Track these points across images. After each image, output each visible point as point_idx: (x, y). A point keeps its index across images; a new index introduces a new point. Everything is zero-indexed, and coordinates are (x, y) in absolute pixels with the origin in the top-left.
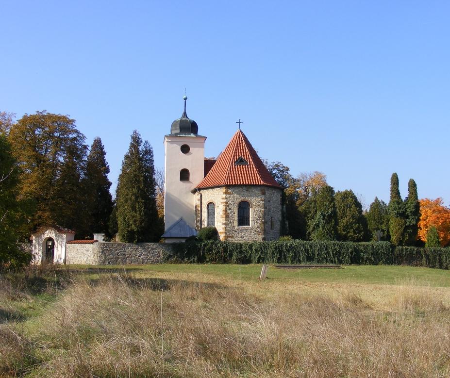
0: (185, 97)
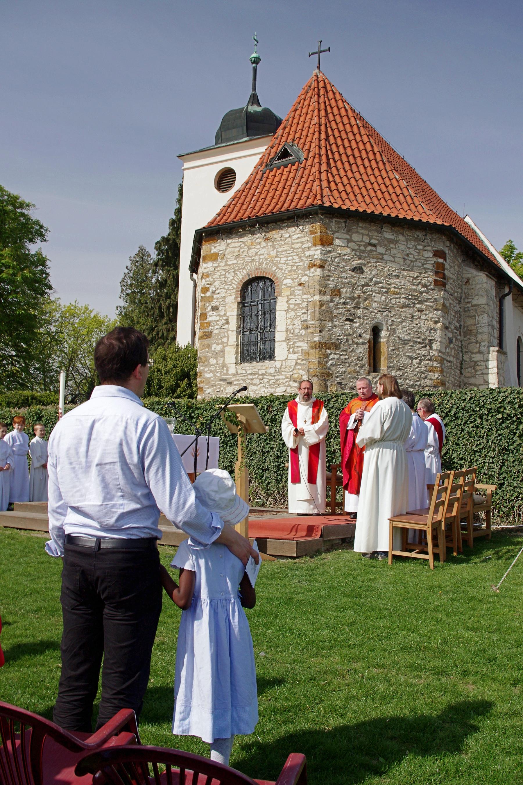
0: (254, 55)
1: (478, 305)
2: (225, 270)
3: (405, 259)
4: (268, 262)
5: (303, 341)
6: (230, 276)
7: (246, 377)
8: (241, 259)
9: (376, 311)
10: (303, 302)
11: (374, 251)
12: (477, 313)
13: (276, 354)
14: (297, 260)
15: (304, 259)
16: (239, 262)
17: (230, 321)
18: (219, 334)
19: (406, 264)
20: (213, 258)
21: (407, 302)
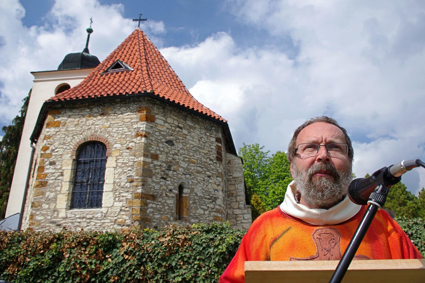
1: (237, 177)
2: (65, 134)
3: (199, 140)
4: (102, 130)
5: (128, 191)
6: (69, 139)
7: (74, 220)
8: (80, 127)
9: (181, 174)
10: (129, 161)
11: (181, 131)
12: (236, 182)
13: (103, 202)
14: (126, 131)
15: (132, 130)
16: (77, 129)
17: (64, 174)
18: (53, 184)
19: (200, 144)
20: (56, 124)
21: (201, 170)
